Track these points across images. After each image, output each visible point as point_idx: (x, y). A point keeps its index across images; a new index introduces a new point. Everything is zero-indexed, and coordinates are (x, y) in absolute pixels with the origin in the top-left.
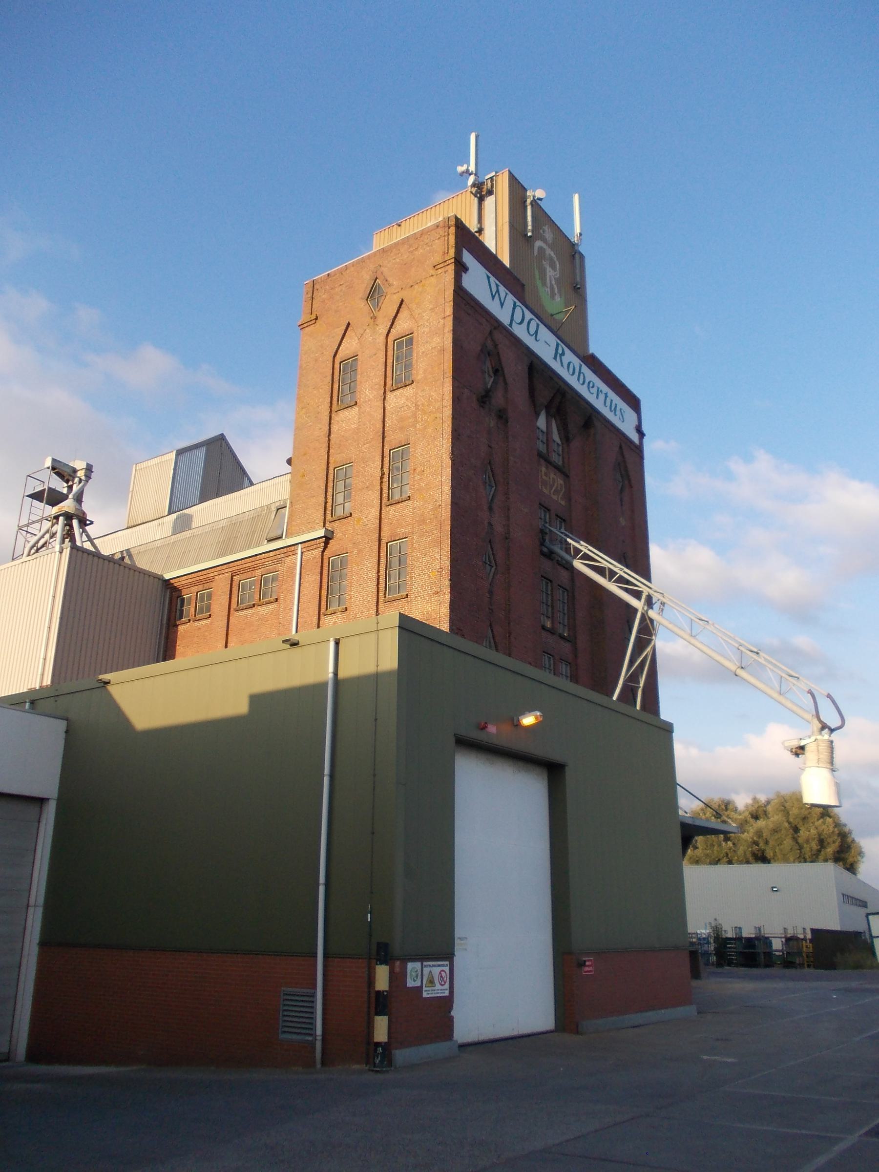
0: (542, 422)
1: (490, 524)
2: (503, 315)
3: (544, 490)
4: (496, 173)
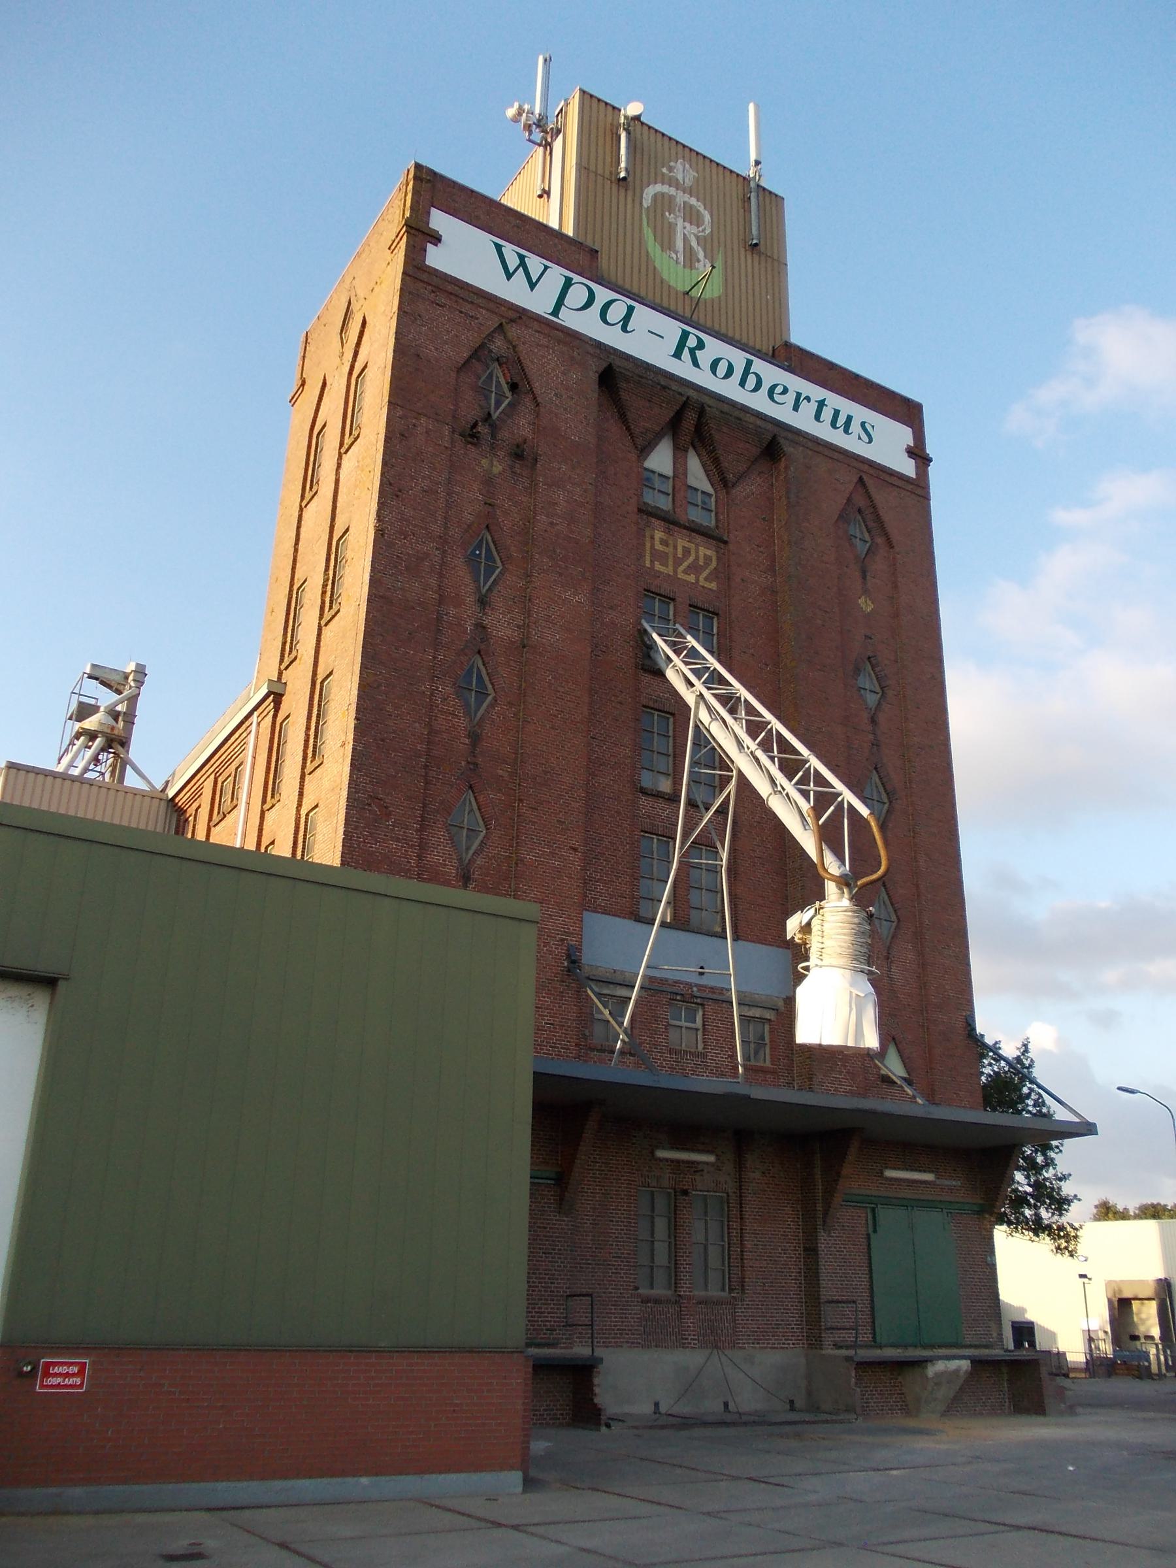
0: (661, 459)
1: (480, 627)
2: (539, 302)
3: (658, 566)
4: (566, 100)
